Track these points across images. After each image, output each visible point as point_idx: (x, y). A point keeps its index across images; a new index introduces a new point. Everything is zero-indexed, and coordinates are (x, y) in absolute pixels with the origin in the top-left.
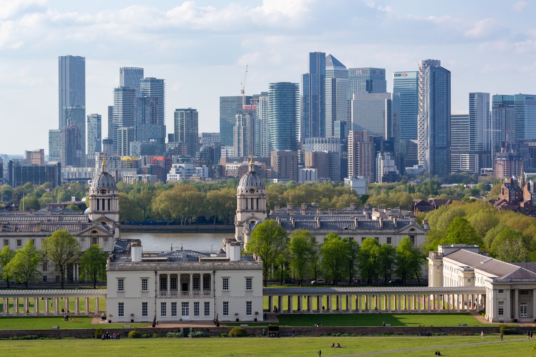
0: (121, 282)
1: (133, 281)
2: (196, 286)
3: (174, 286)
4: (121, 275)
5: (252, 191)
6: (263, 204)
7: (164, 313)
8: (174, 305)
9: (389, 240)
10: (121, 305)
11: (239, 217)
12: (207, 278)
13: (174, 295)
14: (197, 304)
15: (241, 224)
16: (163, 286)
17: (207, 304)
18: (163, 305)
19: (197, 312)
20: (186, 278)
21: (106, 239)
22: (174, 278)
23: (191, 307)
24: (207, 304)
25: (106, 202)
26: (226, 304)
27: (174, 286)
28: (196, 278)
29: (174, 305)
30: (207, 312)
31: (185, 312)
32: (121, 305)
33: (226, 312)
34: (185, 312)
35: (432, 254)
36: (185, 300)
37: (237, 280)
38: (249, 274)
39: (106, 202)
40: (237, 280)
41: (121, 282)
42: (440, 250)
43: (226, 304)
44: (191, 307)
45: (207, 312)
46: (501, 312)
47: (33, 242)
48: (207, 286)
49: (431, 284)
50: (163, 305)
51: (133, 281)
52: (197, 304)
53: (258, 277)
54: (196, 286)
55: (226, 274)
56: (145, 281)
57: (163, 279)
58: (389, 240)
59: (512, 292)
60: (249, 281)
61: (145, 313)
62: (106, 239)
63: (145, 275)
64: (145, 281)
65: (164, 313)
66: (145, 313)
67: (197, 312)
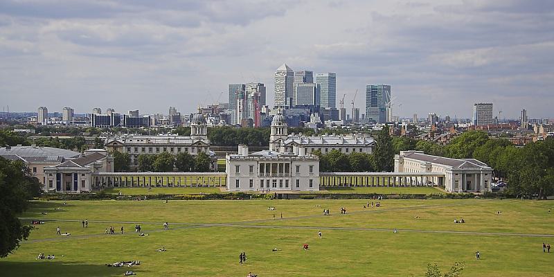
0: (237, 167)
1: (245, 167)
2: (281, 171)
3: (268, 171)
4: (238, 163)
5: (280, 124)
6: (286, 131)
7: (262, 186)
8: (268, 181)
9: (361, 150)
10: (238, 181)
11: (272, 138)
12: (287, 165)
13: (268, 176)
14: (281, 181)
15: (274, 142)
16: (262, 171)
17: (287, 181)
18: (262, 181)
19: (281, 186)
20: (275, 166)
21: (206, 148)
22: (268, 165)
23: (278, 183)
24: (287, 181)
25: (200, 129)
26: (298, 181)
27: (268, 171)
28: (281, 165)
29: (268, 181)
30: (287, 186)
31: (274, 185)
32: (238, 181)
33: (298, 186)
34: (274, 185)
35: (397, 156)
36: (274, 179)
37: (304, 167)
38: (311, 163)
39: (200, 129)
40: (304, 167)
41: (237, 167)
42: (402, 153)
43: (298, 181)
44: (278, 183)
45: (287, 186)
46: (455, 186)
47: (165, 150)
48: (287, 171)
49: (396, 172)
50: (262, 181)
51: (245, 167)
52: (281, 181)
53: (317, 165)
54: (281, 171)
55: (298, 163)
56: (251, 167)
57: (262, 166)
58: (361, 150)
59: (463, 175)
60: (311, 167)
61: (251, 185)
62: (206, 148)
63: (251, 163)
64: (251, 167)
65: (262, 186)
66: (251, 185)
67: (281, 186)
